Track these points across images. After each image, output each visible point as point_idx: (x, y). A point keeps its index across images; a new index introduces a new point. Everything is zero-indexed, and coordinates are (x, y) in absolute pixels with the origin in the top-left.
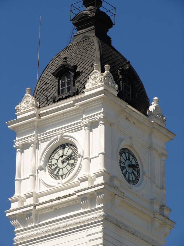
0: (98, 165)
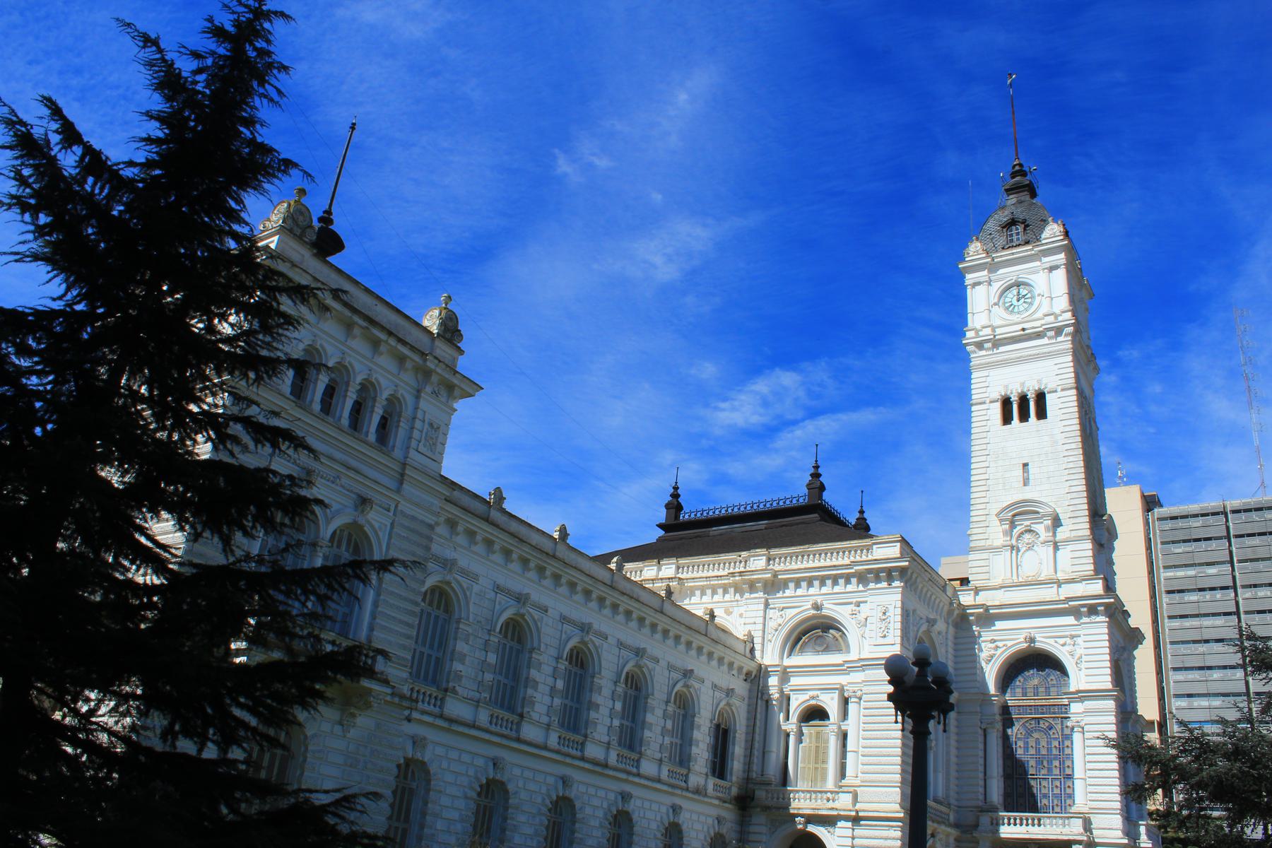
0: (1062, 303)
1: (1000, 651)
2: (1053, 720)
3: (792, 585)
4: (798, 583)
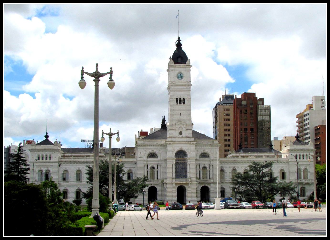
1: (176, 150)
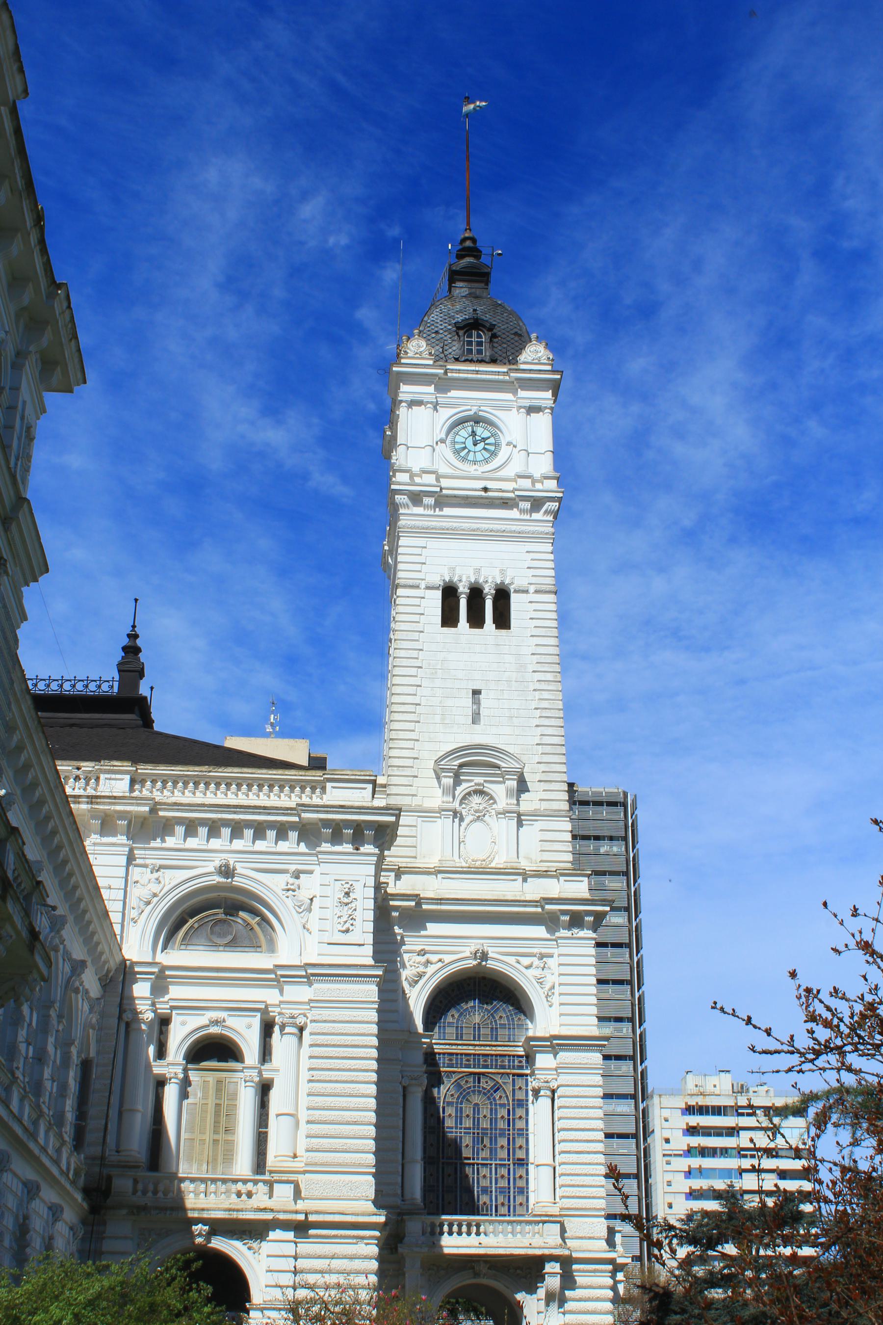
1: (431, 969)
2: (507, 1079)
3: (180, 830)
4: (191, 828)
